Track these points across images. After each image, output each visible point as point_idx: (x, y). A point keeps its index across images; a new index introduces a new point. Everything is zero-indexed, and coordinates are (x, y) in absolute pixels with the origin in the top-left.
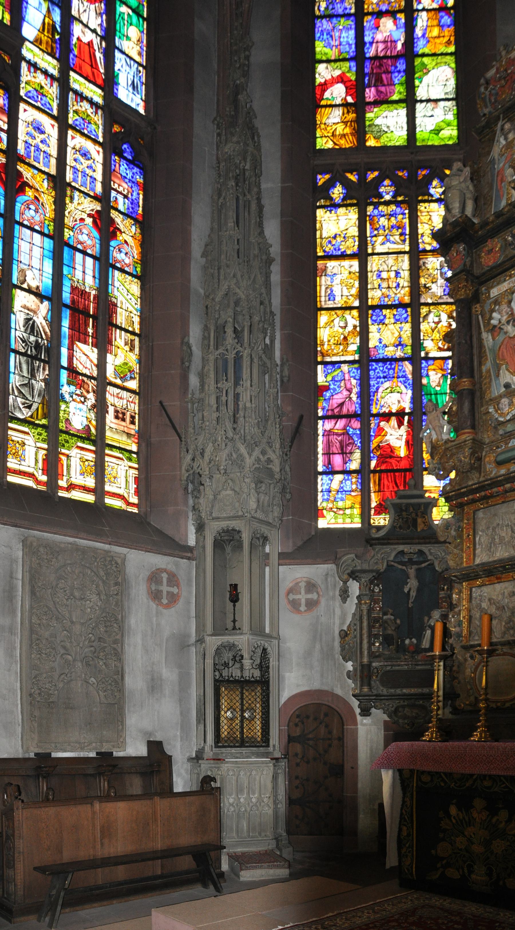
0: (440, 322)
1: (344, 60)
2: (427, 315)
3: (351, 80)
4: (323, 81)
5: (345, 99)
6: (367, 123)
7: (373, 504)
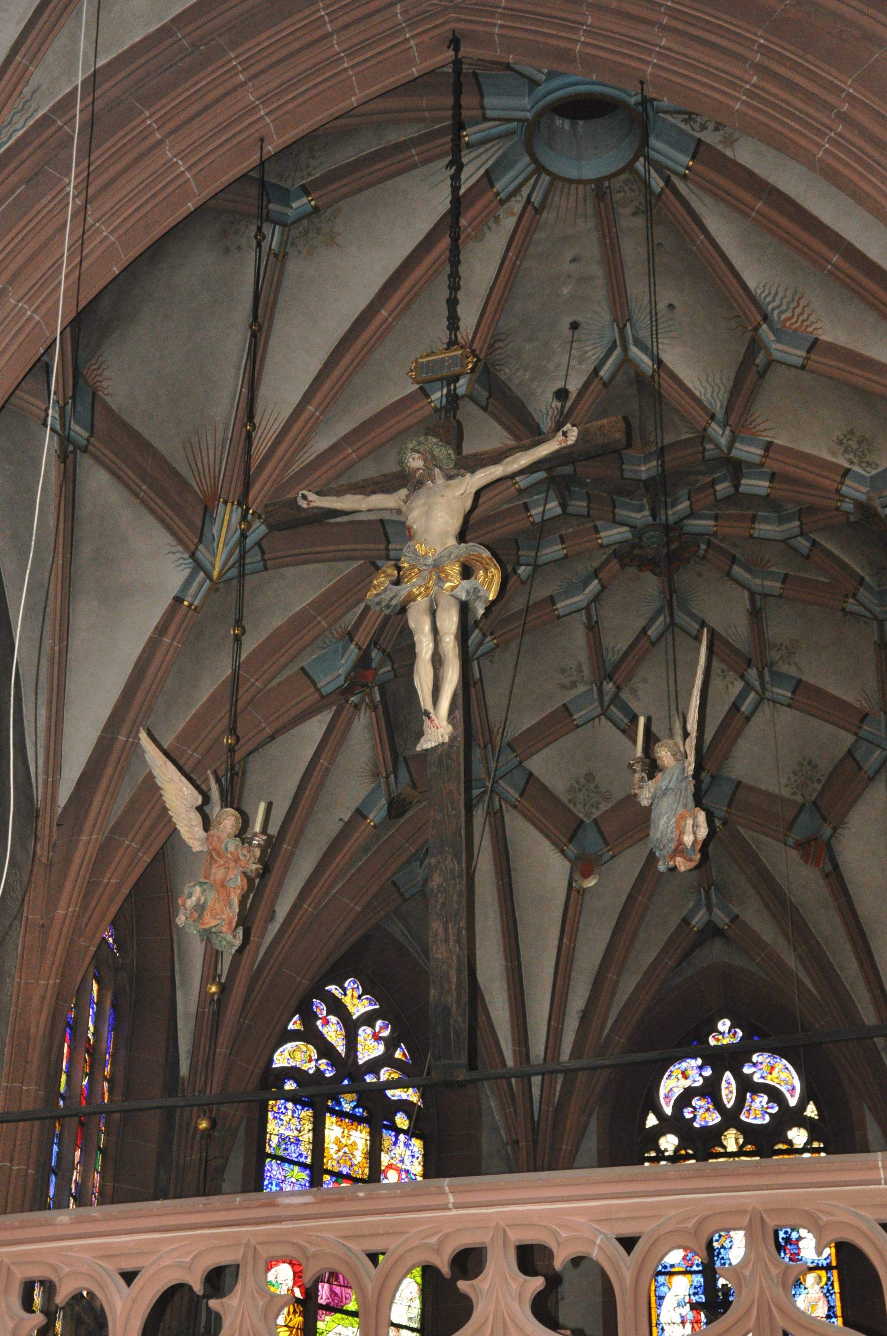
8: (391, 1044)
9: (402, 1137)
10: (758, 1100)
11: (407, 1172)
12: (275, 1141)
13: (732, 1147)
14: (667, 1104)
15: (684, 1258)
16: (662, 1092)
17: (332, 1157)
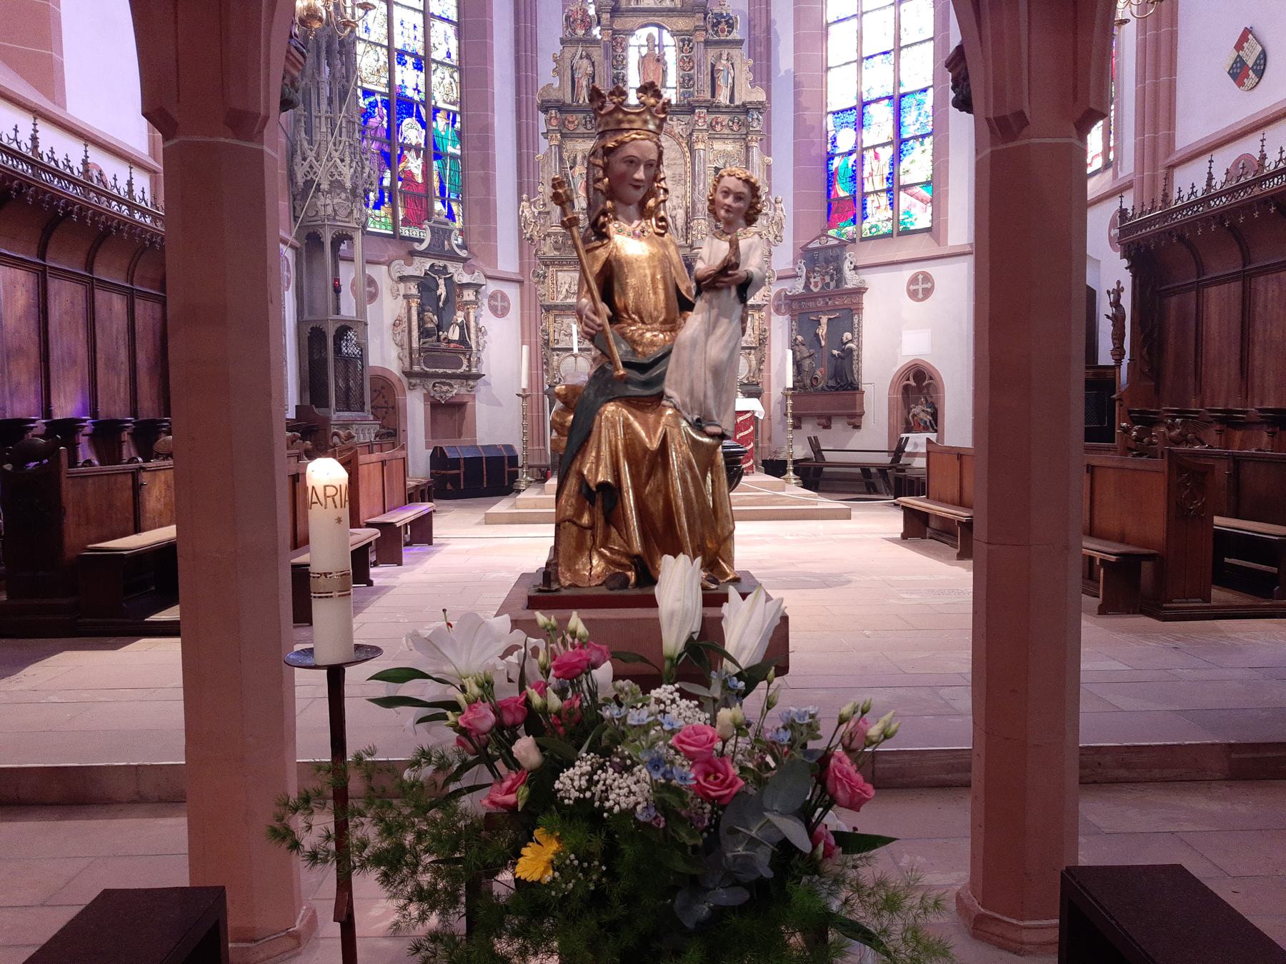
0: (443, 79)
2: (436, 70)
7: (401, 218)
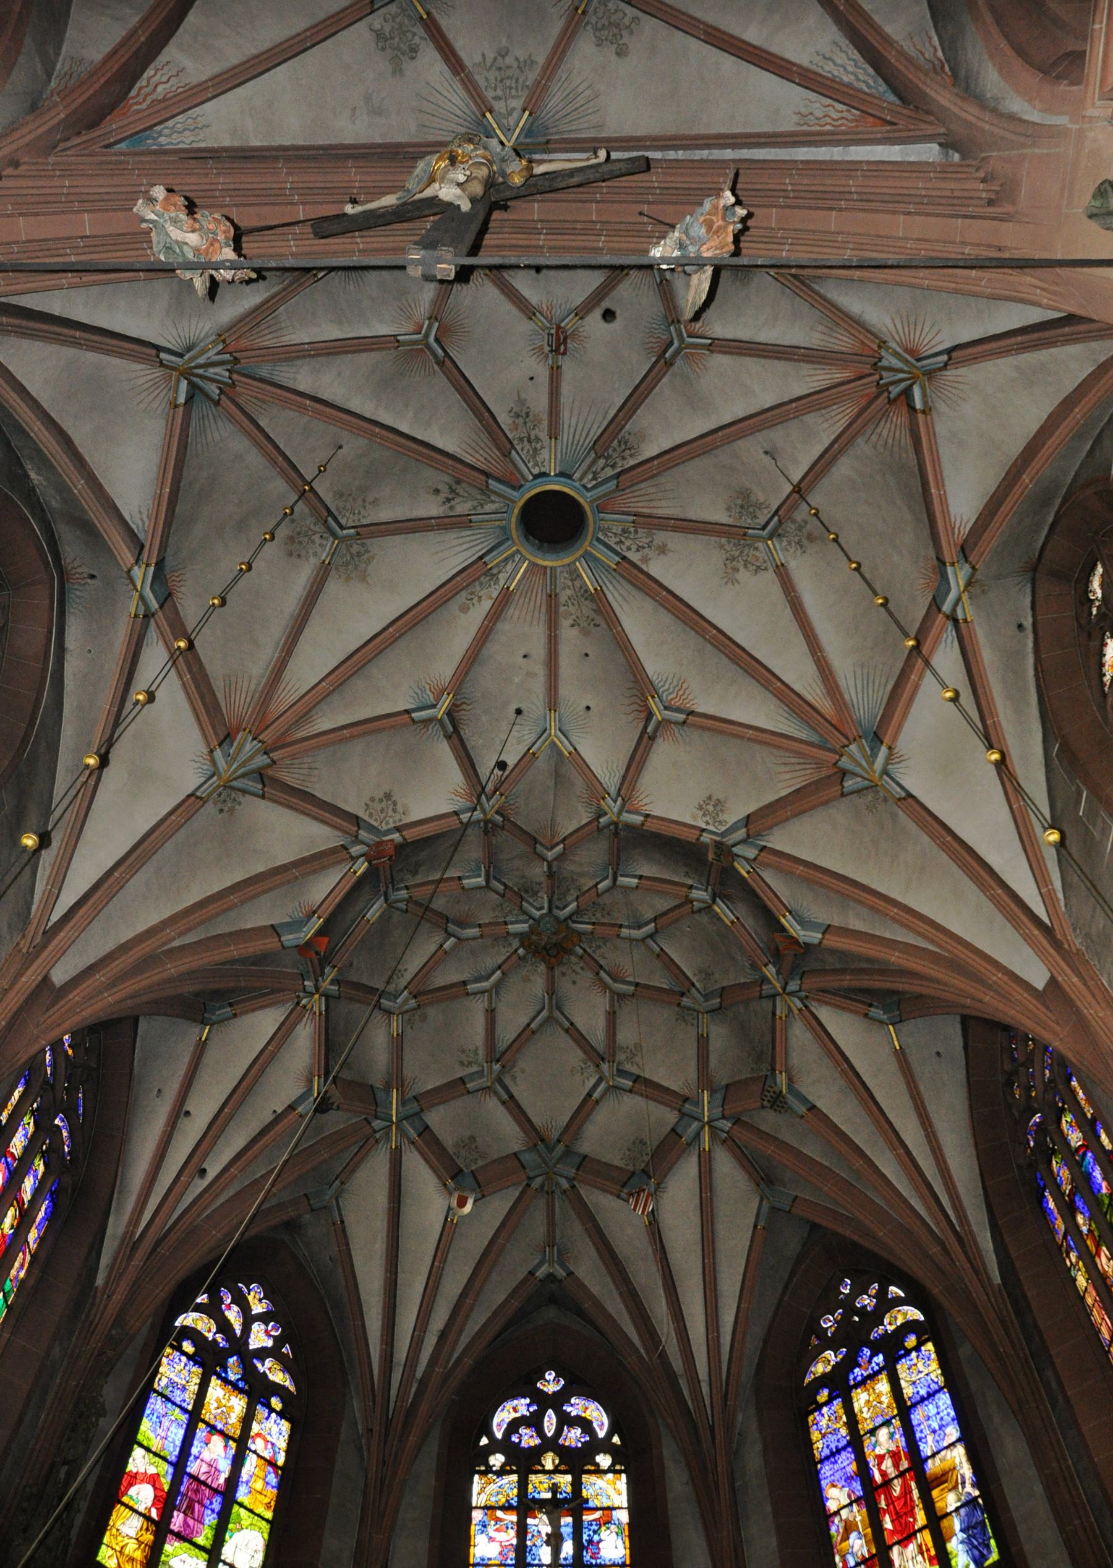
1: (164, 1459)
3: (163, 1490)
4: (135, 1470)
5: (150, 1511)
6: (163, 1558)
8: (279, 1342)
9: (273, 1415)
10: (573, 1431)
11: (273, 1444)
12: (164, 1381)
13: (549, 1466)
14: (499, 1430)
15: (500, 1553)
16: (496, 1421)
17: (210, 1411)
